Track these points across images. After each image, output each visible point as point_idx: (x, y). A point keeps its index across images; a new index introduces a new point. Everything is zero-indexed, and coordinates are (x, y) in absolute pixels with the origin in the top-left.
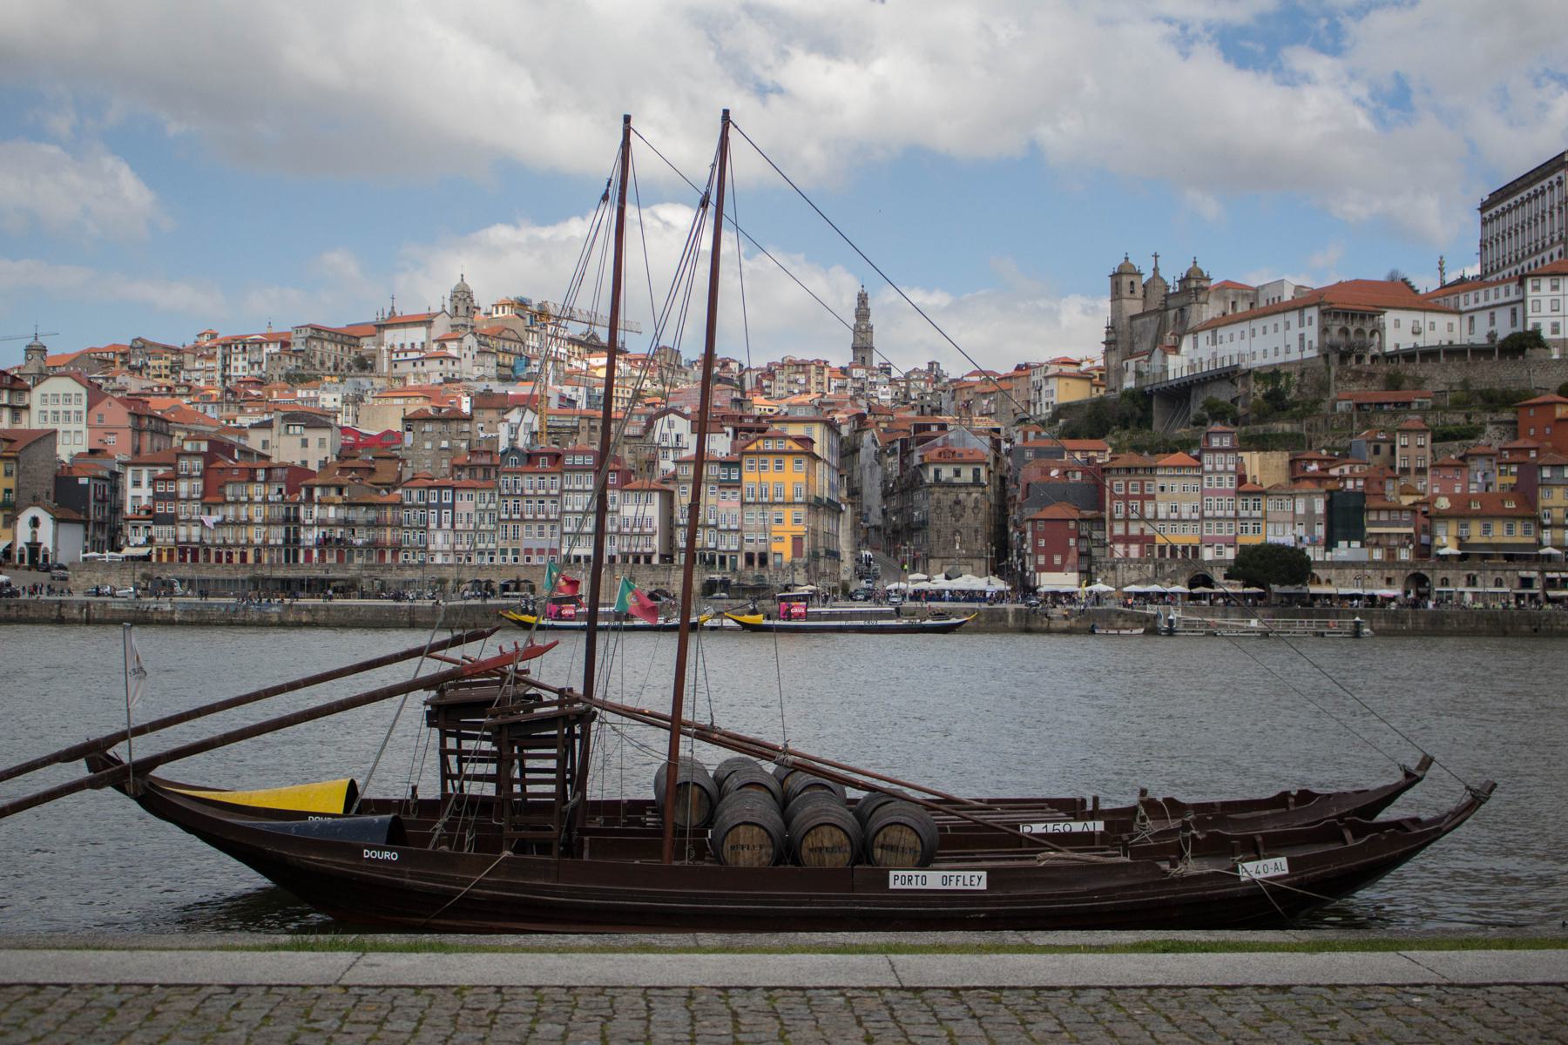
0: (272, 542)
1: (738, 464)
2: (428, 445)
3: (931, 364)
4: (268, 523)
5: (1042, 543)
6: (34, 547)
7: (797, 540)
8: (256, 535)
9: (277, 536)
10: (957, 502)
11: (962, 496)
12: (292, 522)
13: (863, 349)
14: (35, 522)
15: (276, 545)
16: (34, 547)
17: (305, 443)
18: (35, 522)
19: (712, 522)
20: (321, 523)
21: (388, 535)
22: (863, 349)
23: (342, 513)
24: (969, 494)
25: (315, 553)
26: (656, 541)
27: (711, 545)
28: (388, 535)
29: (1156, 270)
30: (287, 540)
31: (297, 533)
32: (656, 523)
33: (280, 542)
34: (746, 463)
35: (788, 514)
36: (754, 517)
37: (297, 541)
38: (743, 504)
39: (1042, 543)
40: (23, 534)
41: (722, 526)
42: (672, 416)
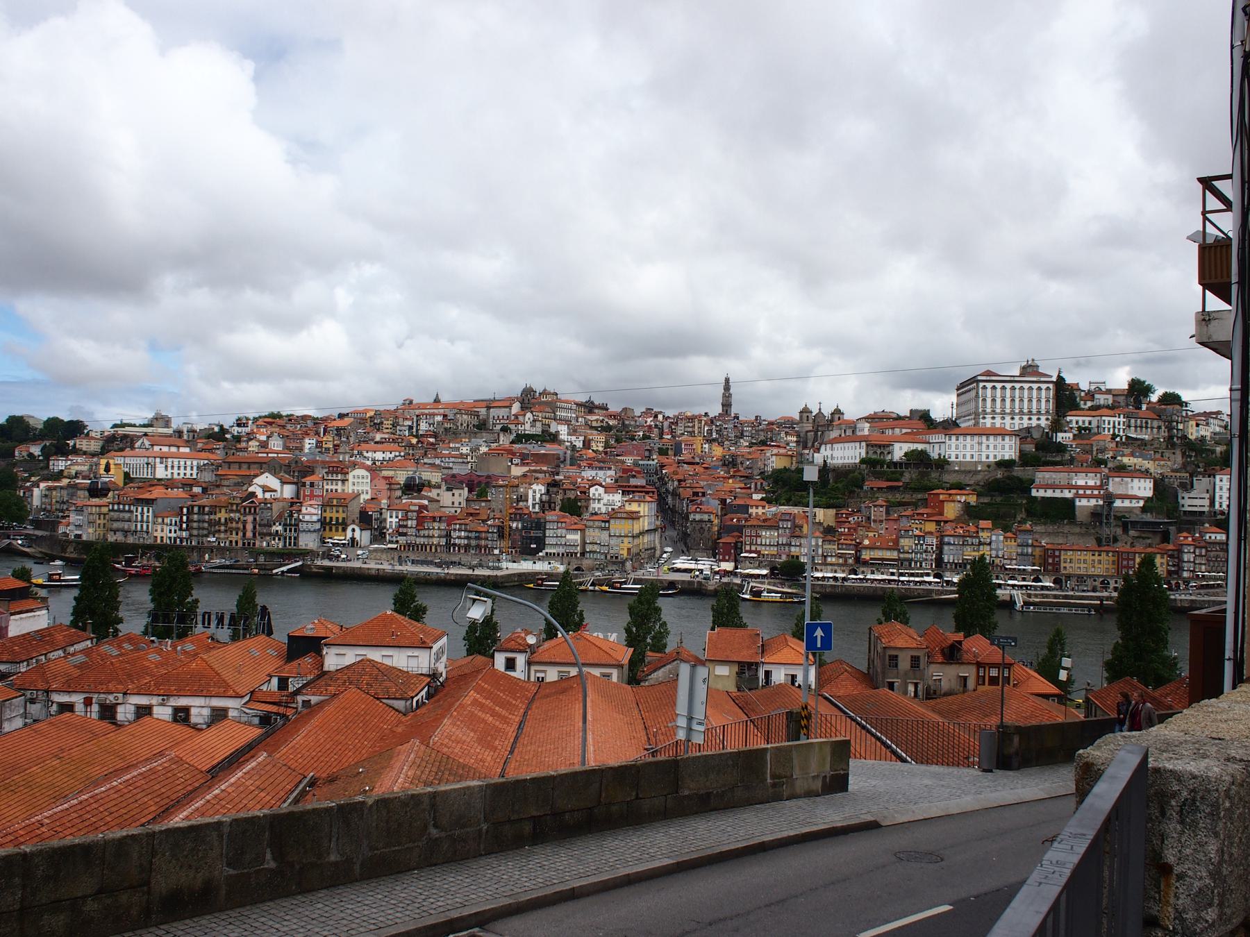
4: (440, 537)
6: (353, 539)
7: (629, 549)
8: (435, 541)
9: (443, 541)
12: (448, 536)
14: (353, 530)
16: (353, 539)
18: (353, 530)
20: (459, 538)
21: (483, 543)
22: (727, 405)
28: (483, 543)
34: (612, 521)
36: (613, 541)
40: (349, 534)
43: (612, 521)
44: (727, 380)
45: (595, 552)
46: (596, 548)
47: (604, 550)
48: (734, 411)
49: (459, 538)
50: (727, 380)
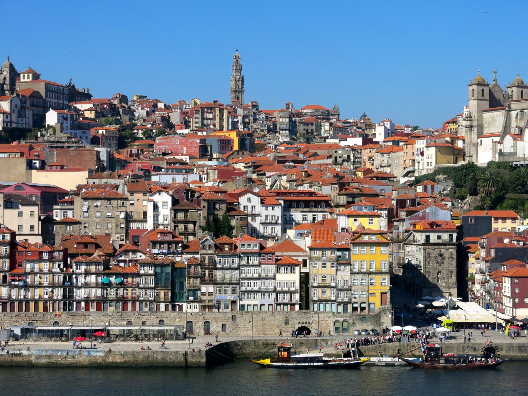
0: (55, 298)
1: (348, 250)
2: (98, 214)
3: (288, 105)
4: (53, 285)
5: (517, 291)
9: (59, 294)
10: (441, 255)
11: (443, 251)
13: (238, 91)
15: (57, 300)
17: (20, 214)
19: (333, 284)
21: (129, 293)
23: (100, 279)
24: (447, 249)
25: (83, 304)
26: (297, 296)
27: (333, 298)
28: (129, 293)
29: (496, 80)
30: (64, 296)
31: (70, 292)
32: (297, 285)
33: (60, 297)
35: (377, 279)
37: (71, 296)
38: (352, 273)
39: (517, 291)
41: (340, 287)
42: (249, 195)
43: (355, 250)
44: (237, 60)
45: (326, 301)
46: (329, 294)
47: (343, 297)
48: (247, 99)
49: (86, 286)
50: (237, 60)
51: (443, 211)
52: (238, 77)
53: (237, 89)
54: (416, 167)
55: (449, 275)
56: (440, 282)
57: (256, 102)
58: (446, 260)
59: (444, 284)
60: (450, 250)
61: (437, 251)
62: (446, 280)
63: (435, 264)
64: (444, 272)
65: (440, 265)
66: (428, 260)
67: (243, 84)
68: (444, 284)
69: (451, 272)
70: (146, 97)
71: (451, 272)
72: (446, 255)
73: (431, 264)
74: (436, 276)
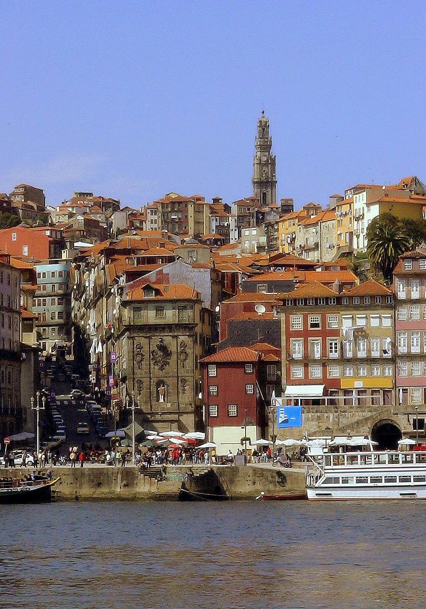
11: (168, 340)
44: (264, 128)
50: (264, 128)
51: (196, 270)
52: (265, 159)
53: (263, 179)
54: (355, 246)
55: (180, 388)
56: (162, 400)
57: (291, 200)
58: (174, 357)
59: (169, 405)
60: (181, 338)
61: (156, 341)
62: (173, 398)
63: (152, 366)
64: (171, 381)
65: (162, 369)
66: (139, 358)
67: (273, 170)
68: (169, 405)
69: (184, 381)
70: (91, 194)
71: (184, 381)
72: (173, 348)
73: (144, 366)
74: (153, 389)
